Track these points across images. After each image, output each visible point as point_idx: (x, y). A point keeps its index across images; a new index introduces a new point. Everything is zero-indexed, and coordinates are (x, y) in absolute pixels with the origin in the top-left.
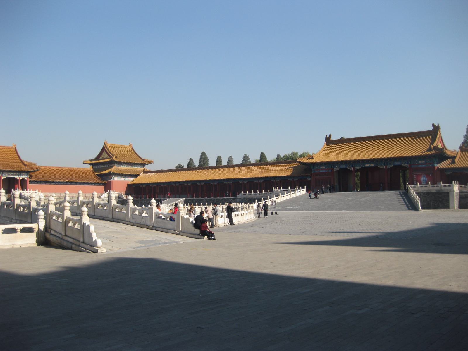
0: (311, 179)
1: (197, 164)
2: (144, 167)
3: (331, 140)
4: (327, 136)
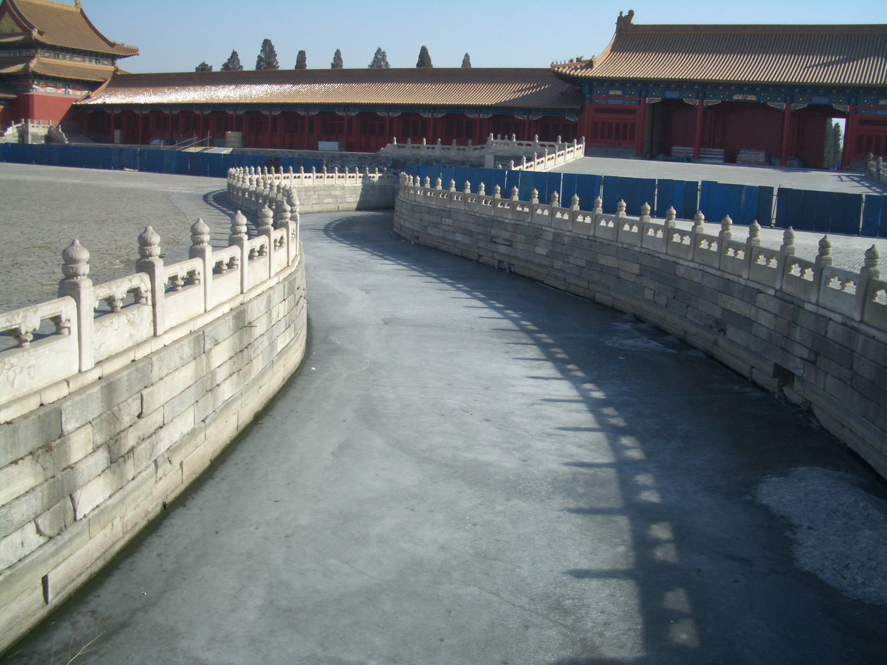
0: (577, 119)
1: (249, 63)
2: (113, 64)
3: (632, 25)
4: (621, 13)
